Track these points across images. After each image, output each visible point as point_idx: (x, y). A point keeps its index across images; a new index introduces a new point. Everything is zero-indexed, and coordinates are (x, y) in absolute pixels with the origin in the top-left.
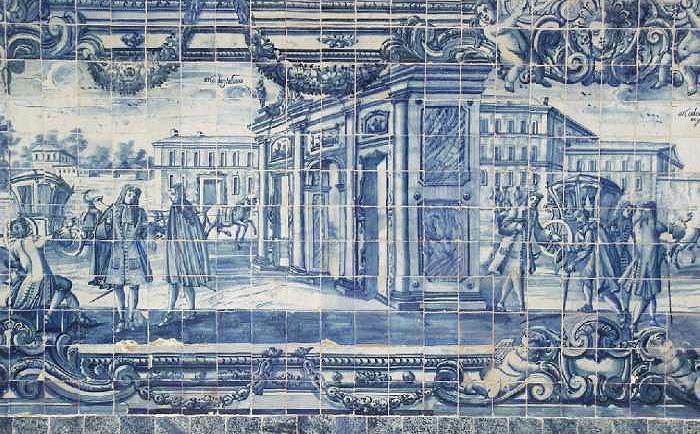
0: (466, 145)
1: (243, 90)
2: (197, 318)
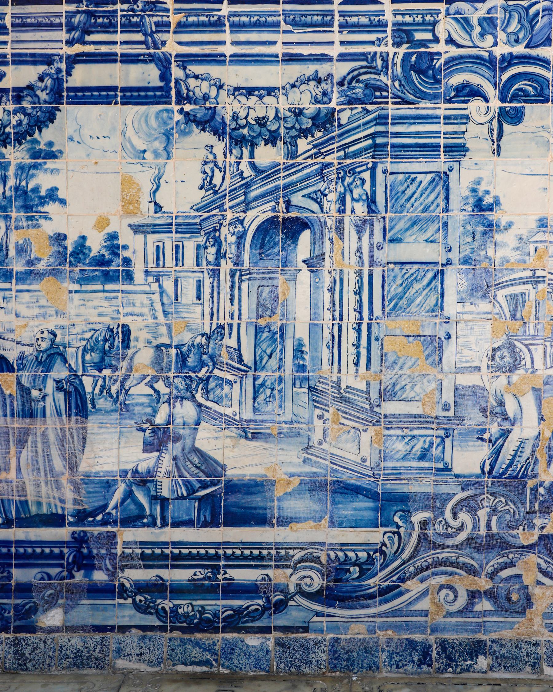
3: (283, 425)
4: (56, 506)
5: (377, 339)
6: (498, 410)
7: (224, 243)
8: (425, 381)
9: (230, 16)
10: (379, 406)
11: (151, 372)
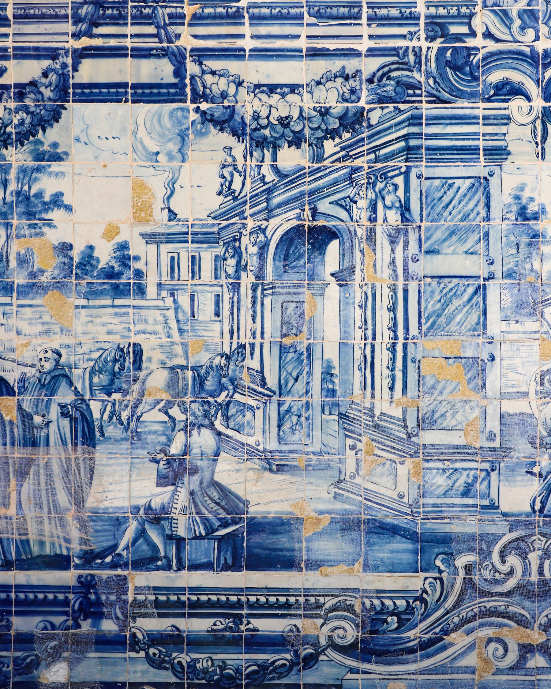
3: (311, 456)
4: (60, 546)
5: (414, 361)
7: (244, 254)
8: (468, 407)
9: (249, 8)
11: (165, 396)
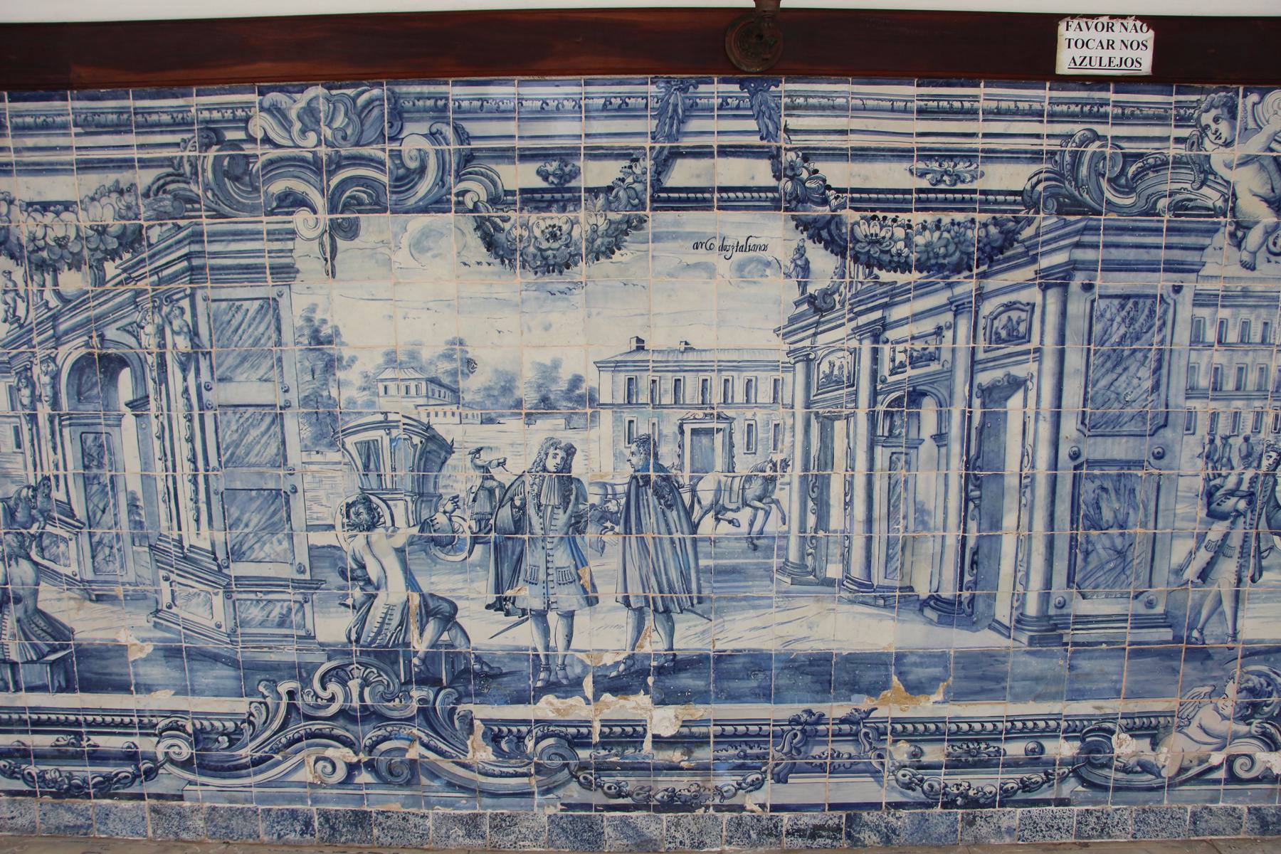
0: (1165, 364)
1: (768, 264)
2: (676, 665)
3: (128, 587)
5: (216, 493)
6: (359, 573)
10: (228, 567)
